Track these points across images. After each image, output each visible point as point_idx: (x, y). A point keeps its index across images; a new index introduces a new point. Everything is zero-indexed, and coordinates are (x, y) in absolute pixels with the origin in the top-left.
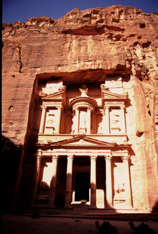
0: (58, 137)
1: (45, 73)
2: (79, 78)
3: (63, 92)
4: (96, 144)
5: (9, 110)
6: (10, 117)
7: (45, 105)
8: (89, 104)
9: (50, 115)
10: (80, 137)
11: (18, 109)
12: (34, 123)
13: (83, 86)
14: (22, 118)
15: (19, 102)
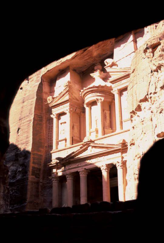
0: (69, 149)
1: (48, 71)
2: (89, 58)
3: (68, 89)
4: (104, 150)
5: (18, 133)
6: (19, 142)
7: (55, 111)
8: (100, 94)
9: (61, 124)
10: (86, 145)
11: (24, 130)
12: (49, 139)
13: (95, 68)
14: (28, 139)
15: (24, 121)
